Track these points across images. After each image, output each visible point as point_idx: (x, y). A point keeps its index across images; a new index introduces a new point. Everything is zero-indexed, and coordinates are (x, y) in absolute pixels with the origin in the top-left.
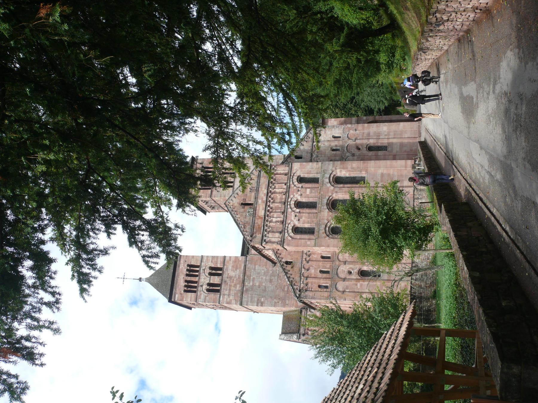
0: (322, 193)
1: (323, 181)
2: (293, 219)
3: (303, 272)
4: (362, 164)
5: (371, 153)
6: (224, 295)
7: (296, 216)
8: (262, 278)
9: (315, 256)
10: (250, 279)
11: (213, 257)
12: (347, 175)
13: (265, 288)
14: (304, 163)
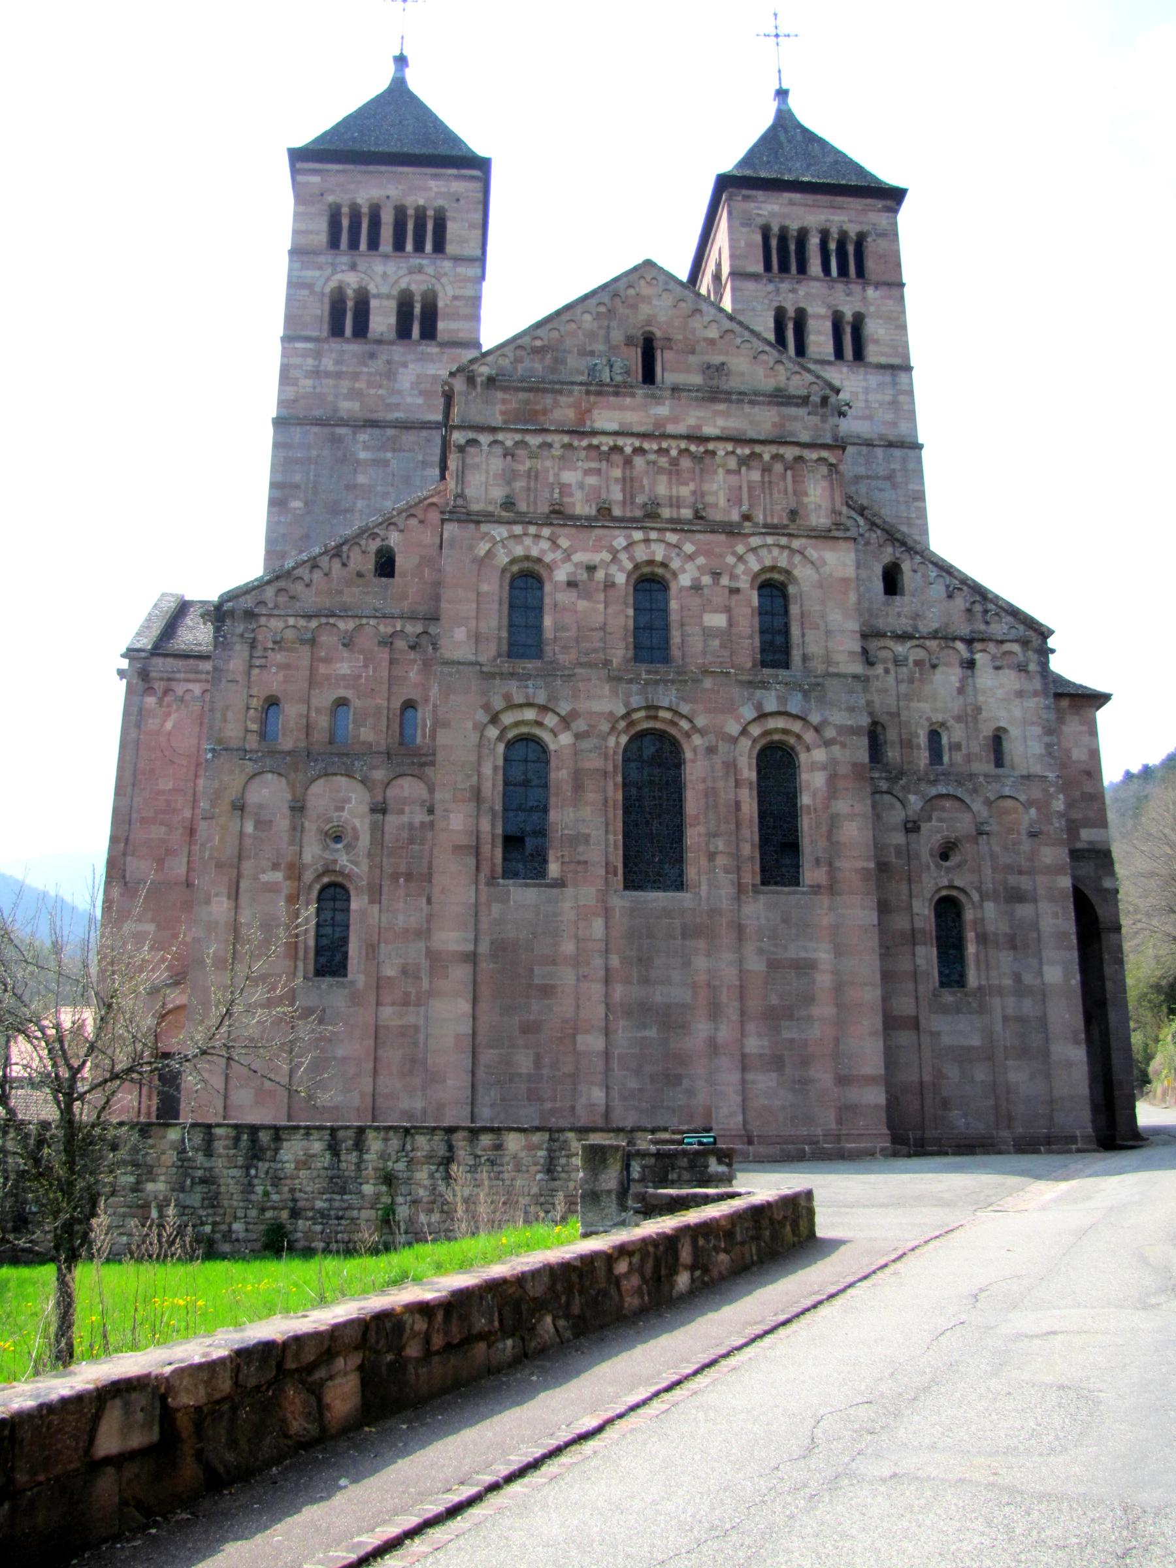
0: (708, 683)
1: (764, 685)
2: (578, 557)
3: (341, 625)
4: (860, 864)
5: (924, 912)
6: (318, 355)
7: (591, 569)
8: (385, 495)
9: (413, 675)
10: (382, 448)
11: (476, 301)
12: (805, 799)
13: (347, 511)
14: (853, 597)
